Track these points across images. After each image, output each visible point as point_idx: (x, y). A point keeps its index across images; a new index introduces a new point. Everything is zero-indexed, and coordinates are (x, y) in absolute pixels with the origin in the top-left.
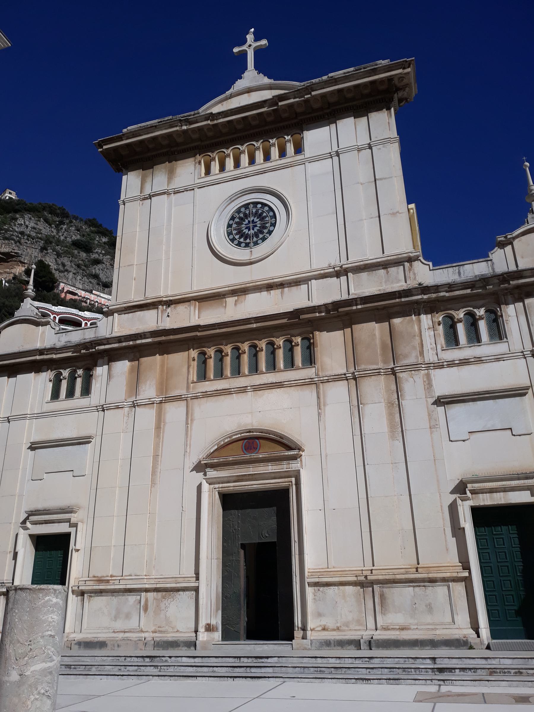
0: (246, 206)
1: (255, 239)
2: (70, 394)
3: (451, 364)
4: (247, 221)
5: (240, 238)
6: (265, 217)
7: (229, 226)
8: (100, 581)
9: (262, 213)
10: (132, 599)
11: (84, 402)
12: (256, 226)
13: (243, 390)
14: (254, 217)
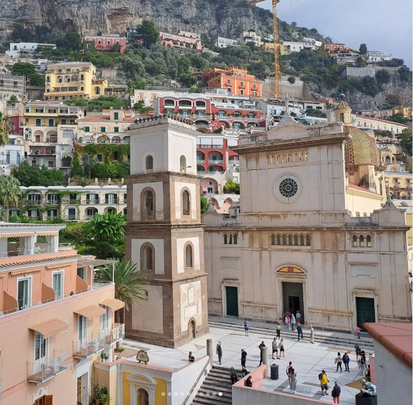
0: (286, 180)
2: (231, 243)
3: (354, 253)
7: (280, 187)
10: (258, 309)
11: (235, 246)
13: (287, 250)
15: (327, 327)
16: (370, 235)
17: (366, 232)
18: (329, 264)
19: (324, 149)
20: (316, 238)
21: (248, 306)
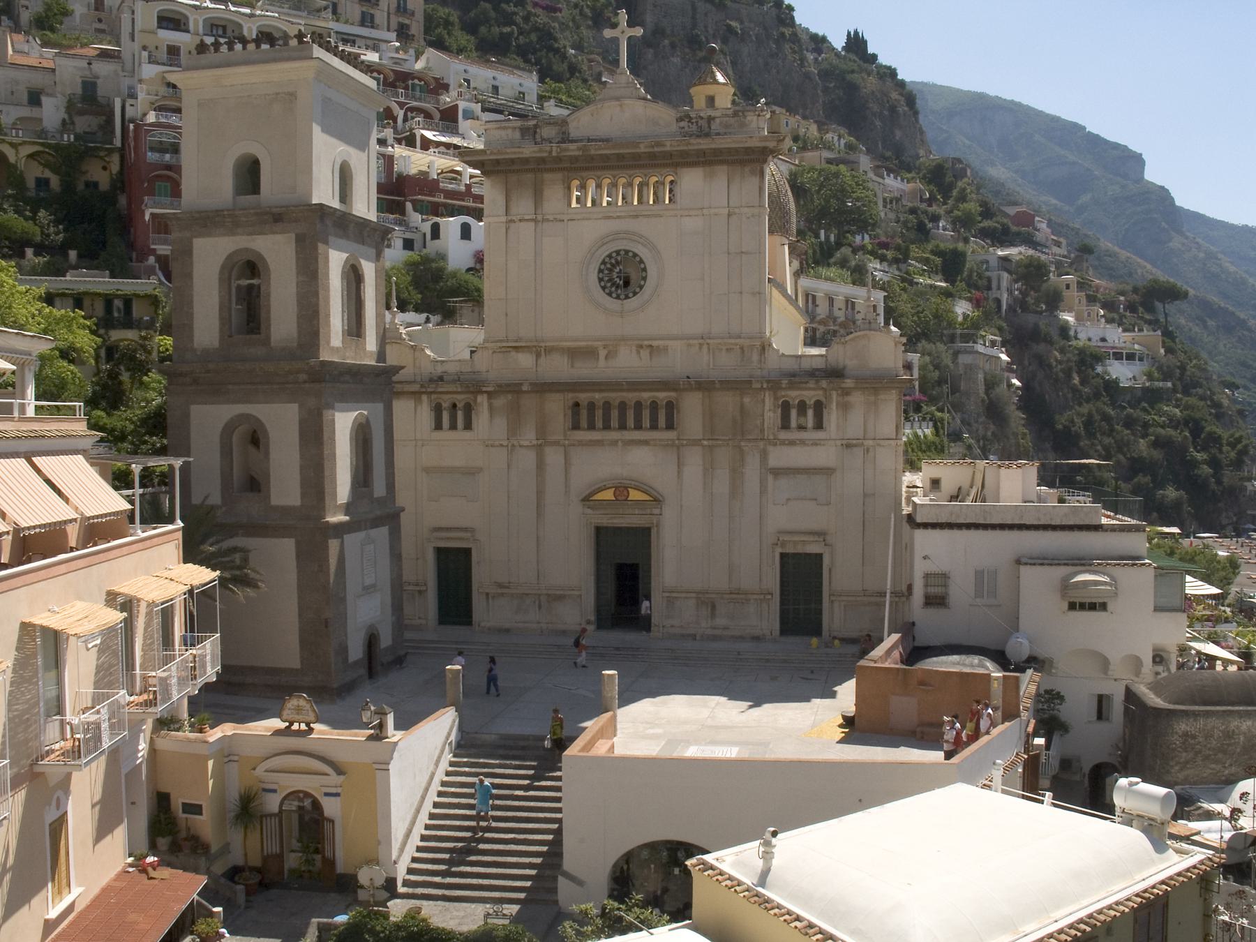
8: (500, 586)
11: (467, 434)
13: (614, 443)
15: (709, 632)
16: (823, 400)
17: (812, 393)
19: (722, 172)
20: (692, 408)
21: (502, 594)
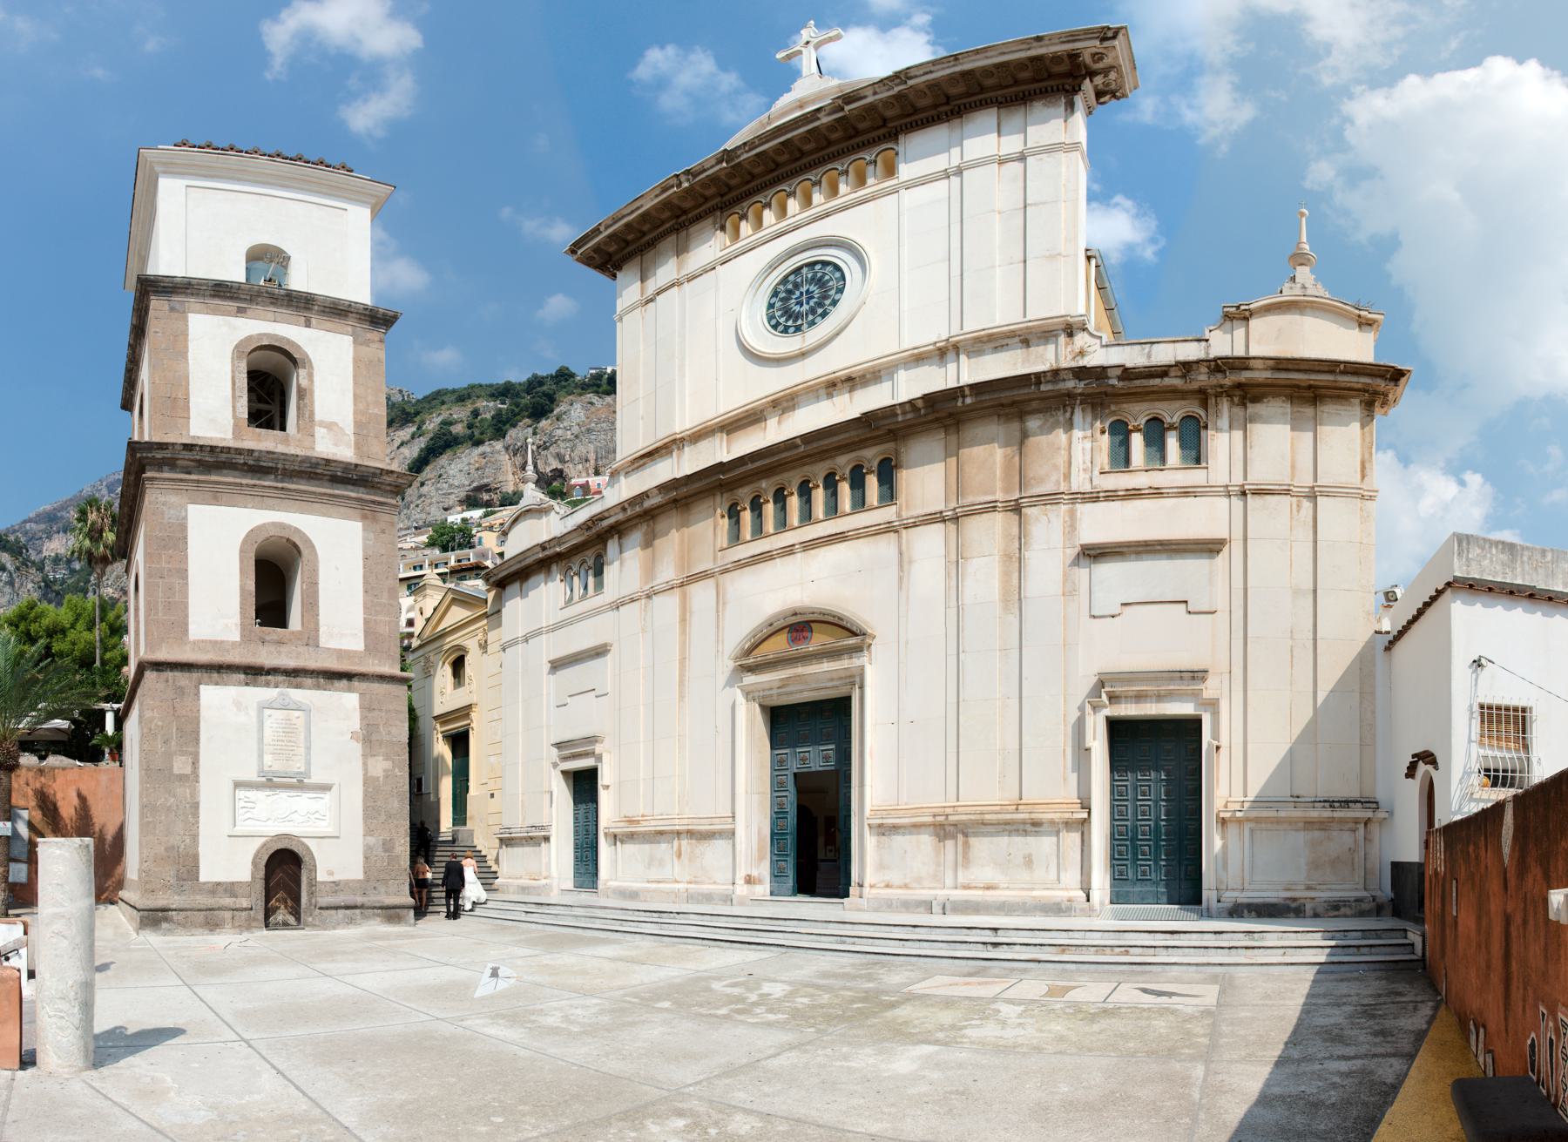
0: (797, 271)
1: (811, 317)
4: (798, 293)
5: (787, 321)
6: (828, 281)
9: (822, 277)
12: (813, 297)
14: (810, 285)
18: (984, 576)
